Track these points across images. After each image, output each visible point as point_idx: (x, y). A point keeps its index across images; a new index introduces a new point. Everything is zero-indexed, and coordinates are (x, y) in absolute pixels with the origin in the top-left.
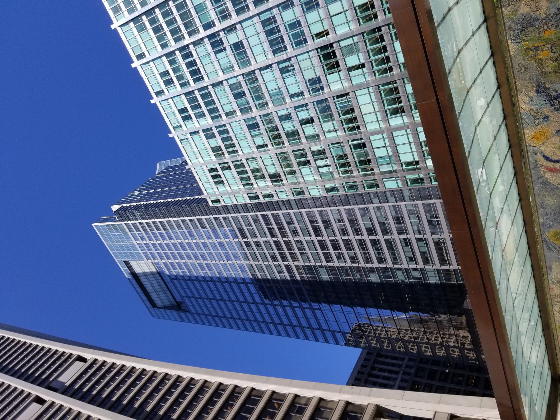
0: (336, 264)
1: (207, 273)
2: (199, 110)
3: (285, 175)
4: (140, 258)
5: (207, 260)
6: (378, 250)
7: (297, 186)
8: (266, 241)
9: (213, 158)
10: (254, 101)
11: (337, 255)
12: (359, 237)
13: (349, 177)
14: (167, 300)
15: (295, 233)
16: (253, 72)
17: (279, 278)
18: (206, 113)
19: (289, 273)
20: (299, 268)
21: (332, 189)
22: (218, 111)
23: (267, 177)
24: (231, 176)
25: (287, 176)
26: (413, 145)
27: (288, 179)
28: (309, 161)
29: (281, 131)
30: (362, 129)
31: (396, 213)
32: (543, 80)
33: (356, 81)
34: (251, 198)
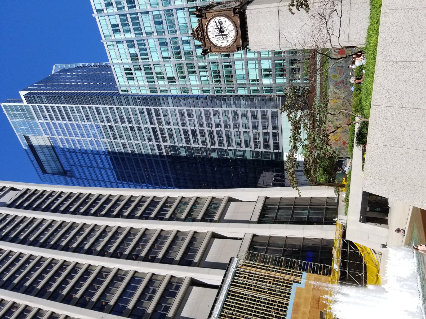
0: (192, 145)
1: (95, 148)
2: (127, 27)
3: (178, 79)
4: (40, 134)
5: (98, 138)
6: (220, 137)
7: (185, 86)
8: (146, 128)
9: (130, 61)
10: (168, 28)
11: (194, 139)
12: (210, 129)
13: (218, 84)
14: (56, 168)
15: (168, 123)
16: (172, 10)
17: (151, 153)
18: (132, 30)
19: (159, 150)
20: (167, 147)
21: (207, 91)
22: (141, 30)
23: (166, 78)
24: (140, 75)
25: (179, 79)
26: (257, 70)
27: (180, 81)
28: (195, 72)
29: (181, 50)
30: (231, 57)
31: (235, 115)
34: (151, 91)
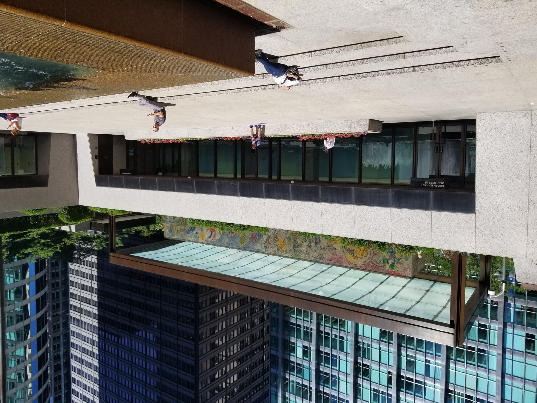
33: (441, 376)
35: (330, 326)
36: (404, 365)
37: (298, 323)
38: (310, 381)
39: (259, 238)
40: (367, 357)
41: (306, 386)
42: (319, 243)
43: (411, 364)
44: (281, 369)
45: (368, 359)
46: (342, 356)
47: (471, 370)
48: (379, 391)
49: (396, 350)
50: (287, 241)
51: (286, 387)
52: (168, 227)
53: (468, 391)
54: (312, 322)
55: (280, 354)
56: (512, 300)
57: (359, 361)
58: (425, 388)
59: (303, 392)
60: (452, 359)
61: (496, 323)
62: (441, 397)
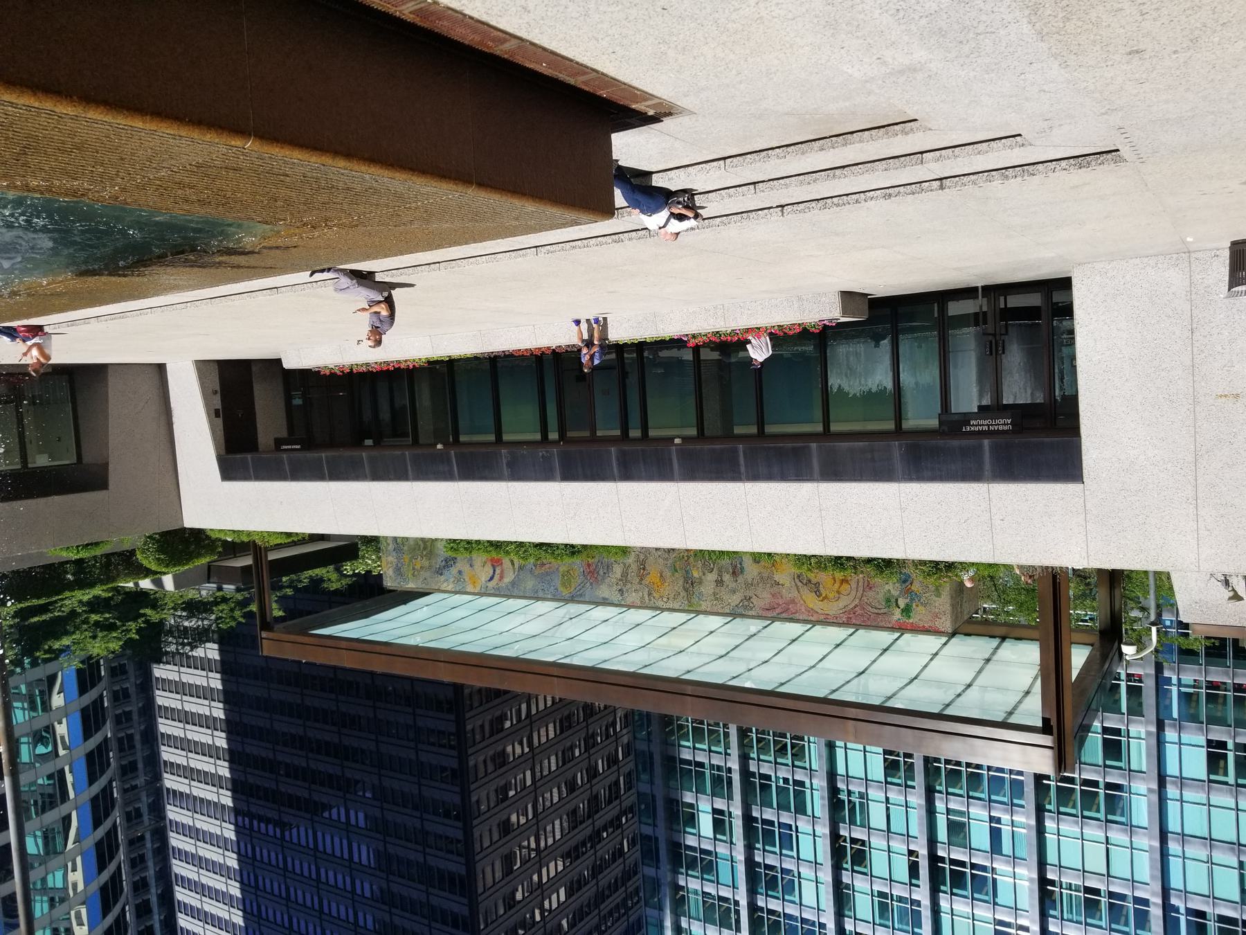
32: (434, 569)
33: (1028, 850)
35: (772, 759)
36: (942, 834)
37: (697, 759)
38: (734, 887)
39: (604, 573)
40: (859, 824)
41: (726, 900)
42: (742, 572)
43: (958, 830)
44: (665, 867)
45: (862, 826)
46: (804, 825)
47: (1094, 832)
48: (892, 895)
49: (923, 802)
50: (667, 573)
51: (679, 904)
52: (392, 563)
53: (1090, 878)
54: (729, 755)
55: (661, 833)
56: (1172, 669)
57: (842, 833)
58: (994, 881)
59: (719, 912)
60: (1050, 811)
61: (1141, 722)
62: (1031, 897)
